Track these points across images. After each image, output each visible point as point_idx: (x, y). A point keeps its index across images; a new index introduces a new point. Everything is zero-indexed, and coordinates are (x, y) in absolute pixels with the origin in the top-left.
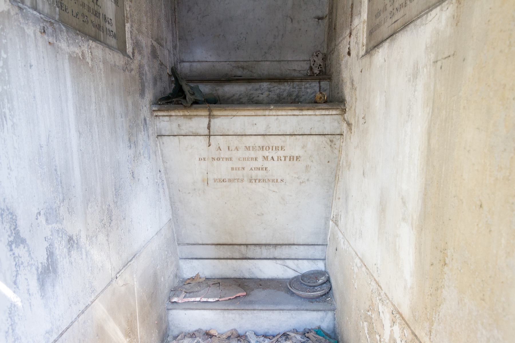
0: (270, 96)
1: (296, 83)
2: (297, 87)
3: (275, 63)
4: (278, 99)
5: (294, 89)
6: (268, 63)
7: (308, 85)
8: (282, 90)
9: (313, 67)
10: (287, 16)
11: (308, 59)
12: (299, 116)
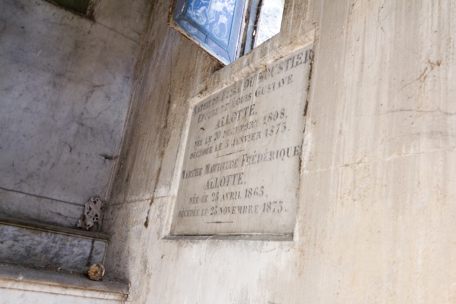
0: (14, 248)
1: (60, 236)
2: (59, 242)
3: (33, 198)
4: (25, 254)
5: (54, 245)
6: (21, 195)
7: (76, 242)
8: (35, 242)
9: (87, 216)
10: (66, 143)
11: (82, 203)
12: (59, 296)
